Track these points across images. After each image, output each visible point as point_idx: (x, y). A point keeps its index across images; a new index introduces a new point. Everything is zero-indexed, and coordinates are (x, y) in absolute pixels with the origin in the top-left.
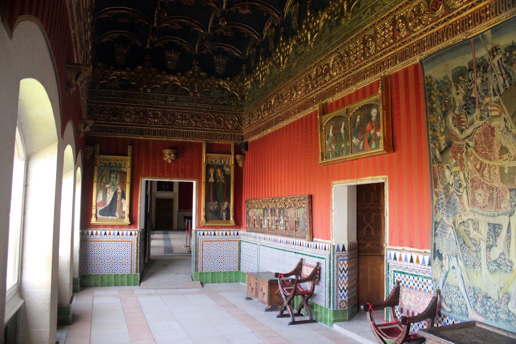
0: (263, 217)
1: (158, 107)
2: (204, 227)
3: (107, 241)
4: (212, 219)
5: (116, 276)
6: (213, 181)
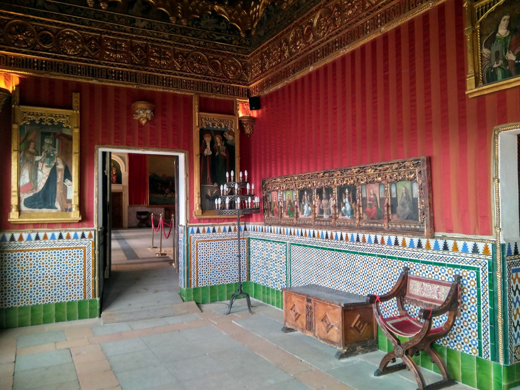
0: (300, 202)
1: (120, 35)
2: (199, 220)
3: (41, 250)
4: (210, 209)
5: (59, 306)
6: (211, 153)
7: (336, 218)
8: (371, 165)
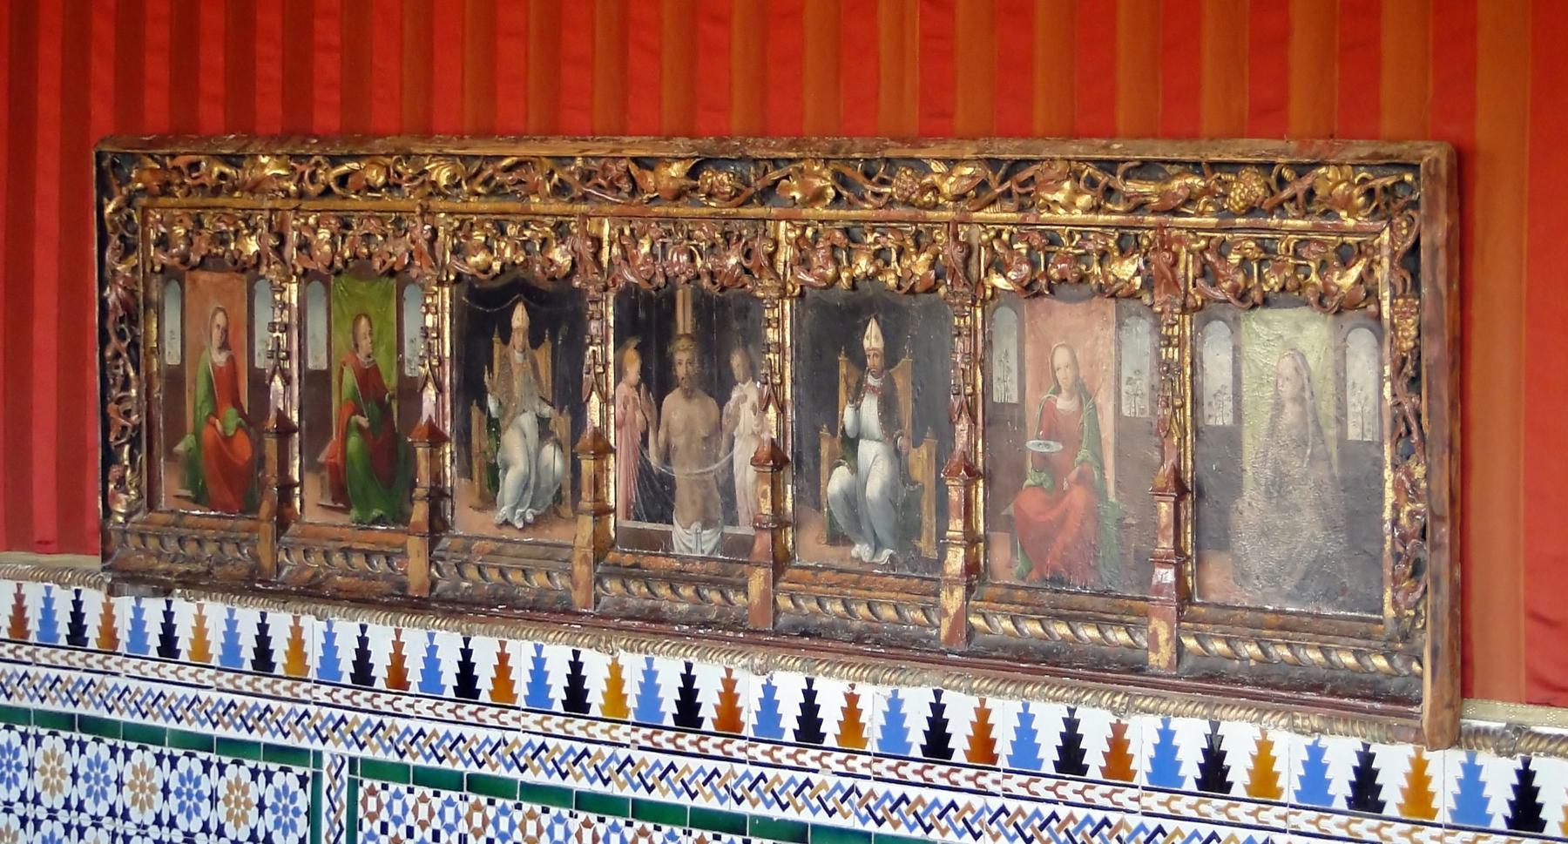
0: (470, 389)
7: (780, 562)
8: (1076, 149)
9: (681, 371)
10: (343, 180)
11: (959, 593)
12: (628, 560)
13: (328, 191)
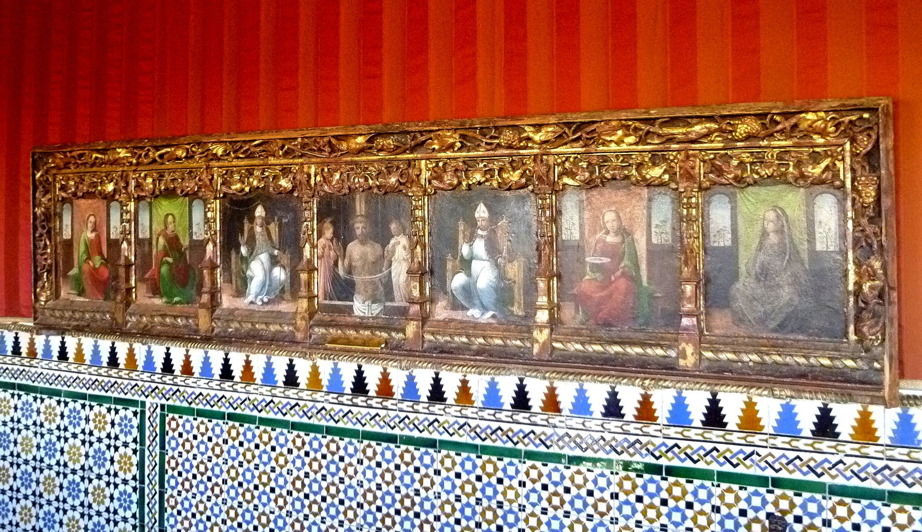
7: (424, 319)
8: (623, 115)
9: (358, 232)
10: (161, 156)
11: (546, 332)
12: (327, 318)
13: (154, 161)
